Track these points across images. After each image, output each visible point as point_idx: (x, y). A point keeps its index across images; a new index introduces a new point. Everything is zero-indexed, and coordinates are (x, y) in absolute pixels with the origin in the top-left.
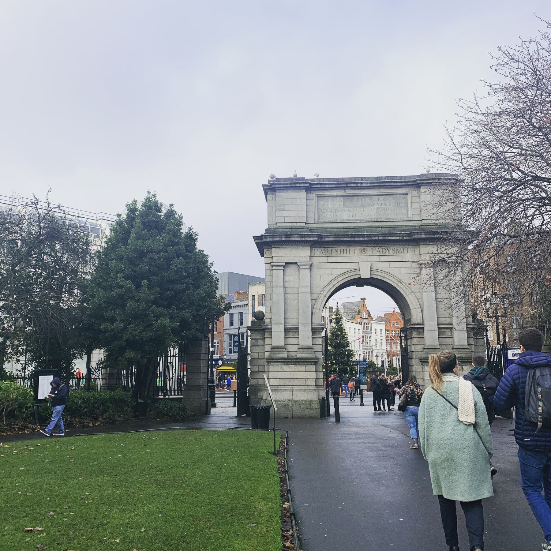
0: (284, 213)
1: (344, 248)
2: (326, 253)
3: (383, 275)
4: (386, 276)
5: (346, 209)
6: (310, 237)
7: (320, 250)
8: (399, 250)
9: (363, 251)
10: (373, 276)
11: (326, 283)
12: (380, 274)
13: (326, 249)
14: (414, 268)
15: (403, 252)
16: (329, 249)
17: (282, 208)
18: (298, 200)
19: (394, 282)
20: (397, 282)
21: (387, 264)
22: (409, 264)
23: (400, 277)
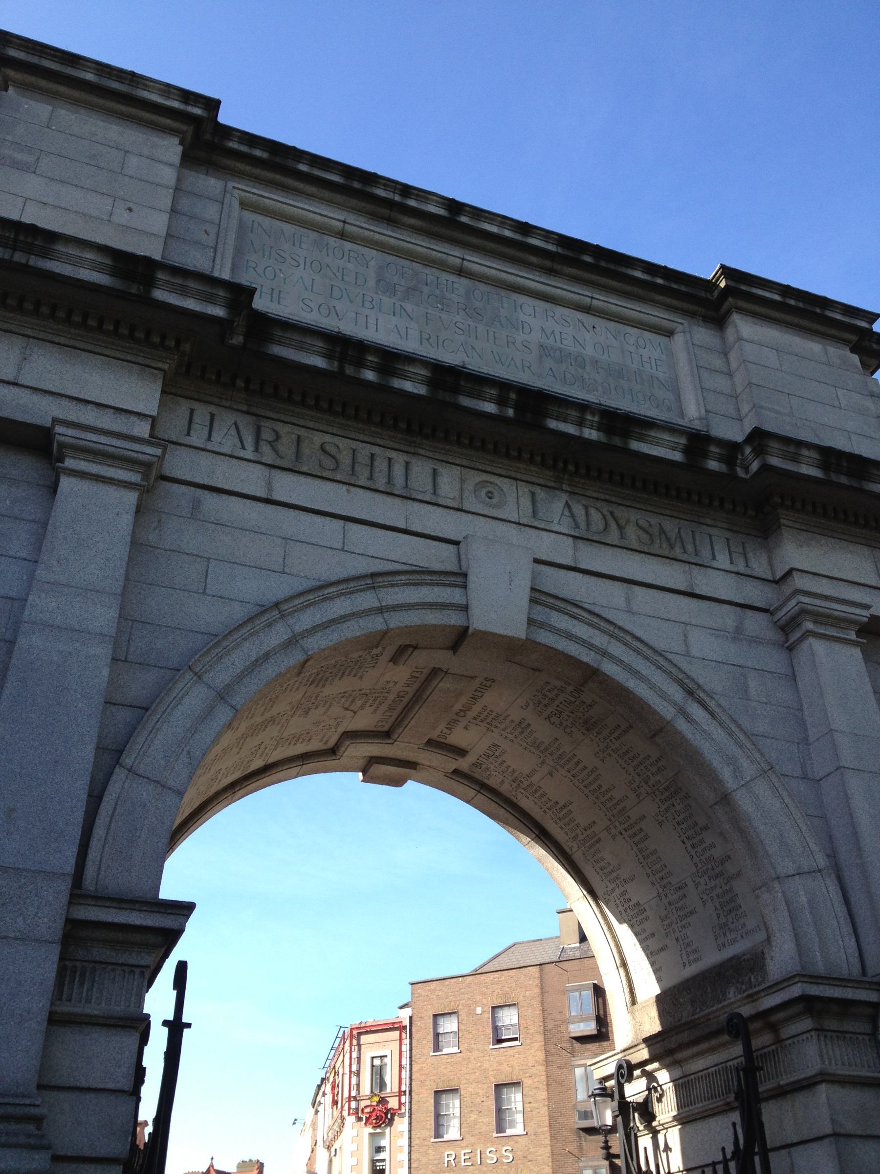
0: (32, 185)
1: (376, 450)
2: (265, 448)
3: (599, 639)
4: (616, 649)
5: (387, 301)
6: (184, 292)
7: (226, 420)
8: (673, 536)
9: (483, 493)
10: (545, 638)
11: (239, 613)
12: (581, 630)
13: (266, 424)
14: (755, 640)
15: (690, 548)
16: (283, 429)
17: (19, 156)
18: (133, 161)
19: (664, 696)
20: (678, 694)
21: (618, 588)
22: (727, 617)
23: (701, 675)
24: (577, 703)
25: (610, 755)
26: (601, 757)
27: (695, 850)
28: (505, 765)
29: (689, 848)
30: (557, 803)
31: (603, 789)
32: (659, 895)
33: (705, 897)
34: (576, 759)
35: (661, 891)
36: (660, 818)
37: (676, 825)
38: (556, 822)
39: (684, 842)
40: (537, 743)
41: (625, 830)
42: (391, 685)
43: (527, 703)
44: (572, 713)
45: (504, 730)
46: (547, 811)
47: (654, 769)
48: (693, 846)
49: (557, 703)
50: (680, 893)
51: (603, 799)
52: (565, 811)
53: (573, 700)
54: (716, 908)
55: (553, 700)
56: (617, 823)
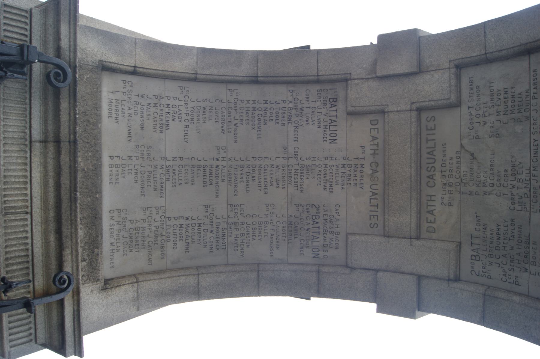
24: (310, 242)
25: (267, 216)
26: (269, 207)
27: (179, 226)
28: (316, 123)
29: (182, 221)
30: (265, 124)
31: (250, 179)
32: (165, 159)
33: (148, 213)
34: (281, 186)
35: (168, 163)
36: (210, 210)
37: (200, 222)
38: (254, 102)
39: (187, 218)
40: (310, 173)
41: (217, 167)
42: (446, 201)
43: (337, 213)
44: (308, 230)
45: (337, 166)
46: (266, 105)
47: (239, 242)
48: (181, 226)
49: (321, 231)
50: (159, 187)
51: (246, 170)
52: (256, 122)
53: (315, 244)
54: (137, 221)
55: (325, 231)
56: (224, 163)
